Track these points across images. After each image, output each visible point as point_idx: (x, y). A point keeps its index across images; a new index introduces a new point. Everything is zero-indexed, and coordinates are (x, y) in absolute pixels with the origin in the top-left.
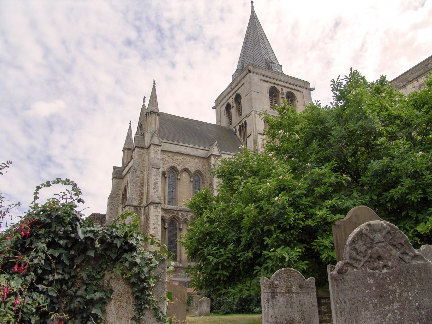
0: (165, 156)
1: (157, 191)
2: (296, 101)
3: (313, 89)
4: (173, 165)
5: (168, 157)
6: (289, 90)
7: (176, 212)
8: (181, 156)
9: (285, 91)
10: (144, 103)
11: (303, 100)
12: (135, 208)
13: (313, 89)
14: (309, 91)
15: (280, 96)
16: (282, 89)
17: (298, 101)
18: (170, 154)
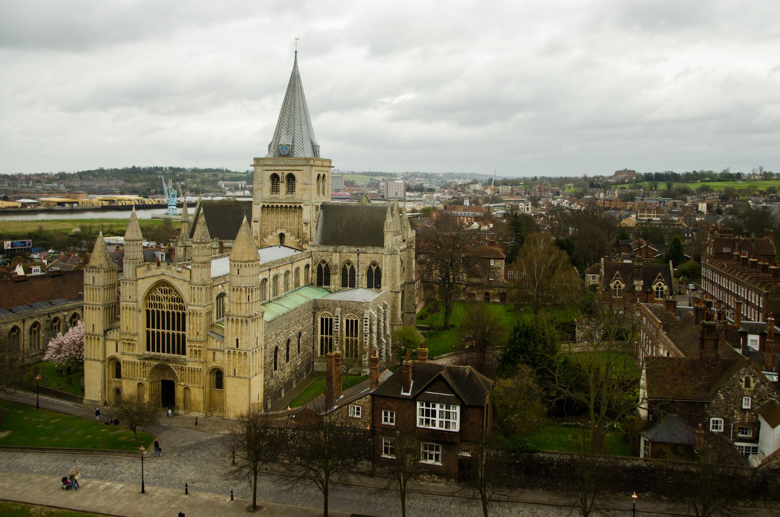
6: (289, 172)
9: (286, 173)
14: (309, 167)
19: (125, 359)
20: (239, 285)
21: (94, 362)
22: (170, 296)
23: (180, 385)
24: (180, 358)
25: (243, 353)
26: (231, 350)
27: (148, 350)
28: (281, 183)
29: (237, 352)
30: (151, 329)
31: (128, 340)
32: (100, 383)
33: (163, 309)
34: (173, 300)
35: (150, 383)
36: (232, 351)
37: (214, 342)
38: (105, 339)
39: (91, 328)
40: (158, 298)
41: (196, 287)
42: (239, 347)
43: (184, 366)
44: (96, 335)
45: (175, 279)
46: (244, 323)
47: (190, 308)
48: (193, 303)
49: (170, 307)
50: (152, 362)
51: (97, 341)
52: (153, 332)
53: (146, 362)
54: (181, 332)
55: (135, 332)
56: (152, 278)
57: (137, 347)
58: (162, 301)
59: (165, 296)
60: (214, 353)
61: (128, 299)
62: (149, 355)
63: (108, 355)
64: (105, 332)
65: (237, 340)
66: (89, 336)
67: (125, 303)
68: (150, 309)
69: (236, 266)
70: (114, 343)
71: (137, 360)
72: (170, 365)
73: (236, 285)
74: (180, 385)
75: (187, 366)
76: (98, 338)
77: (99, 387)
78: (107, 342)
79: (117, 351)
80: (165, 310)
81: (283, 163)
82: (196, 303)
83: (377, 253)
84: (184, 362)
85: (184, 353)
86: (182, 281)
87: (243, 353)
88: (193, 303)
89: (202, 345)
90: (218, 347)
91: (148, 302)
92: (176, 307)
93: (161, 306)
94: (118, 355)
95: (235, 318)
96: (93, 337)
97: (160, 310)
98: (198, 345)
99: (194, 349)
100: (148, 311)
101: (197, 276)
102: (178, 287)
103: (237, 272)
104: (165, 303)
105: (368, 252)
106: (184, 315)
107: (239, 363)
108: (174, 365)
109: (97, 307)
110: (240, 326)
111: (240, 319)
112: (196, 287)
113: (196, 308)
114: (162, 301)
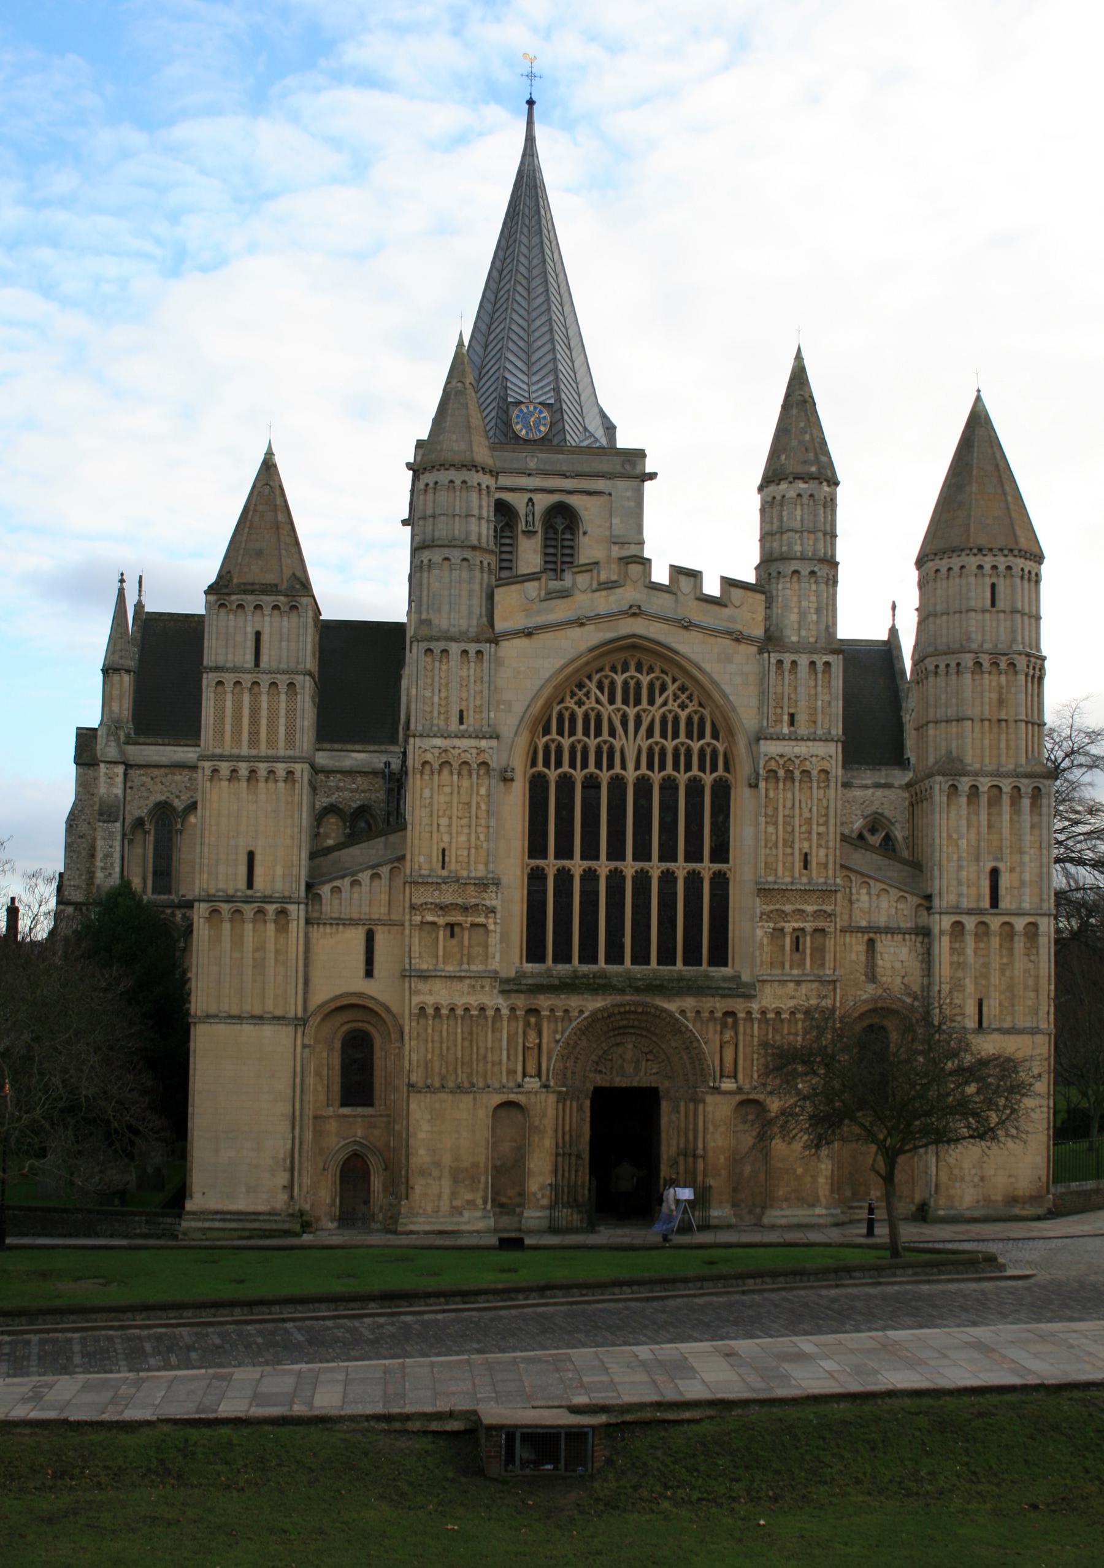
0: (144, 778)
1: (110, 874)
2: (581, 532)
3: (652, 476)
4: (163, 798)
5: (152, 779)
7: (169, 911)
8: (186, 772)
9: (543, 502)
10: (140, 596)
11: (608, 524)
12: (75, 909)
13: (652, 476)
14: (633, 483)
15: (522, 526)
16: (530, 500)
17: (585, 533)
18: (156, 772)
19: (430, 1000)
20: (1002, 647)
21: (247, 1029)
22: (656, 712)
23: (716, 1090)
24: (707, 976)
25: (1020, 924)
26: (964, 919)
27: (534, 952)
28: (520, 536)
29: (995, 923)
30: (551, 865)
31: (443, 908)
32: (284, 1127)
33: (617, 769)
34: (669, 726)
35: (561, 1098)
36: (970, 923)
37: (863, 899)
38: (308, 922)
39: (243, 870)
40: (594, 724)
41: (803, 661)
42: (1005, 903)
43: (739, 1006)
44: (267, 899)
45: (694, 636)
46: (1026, 803)
47: (770, 748)
48: (786, 730)
49: (654, 758)
50: (574, 1002)
51: (271, 927)
52: (564, 877)
53: (544, 1002)
54: (707, 868)
55: (480, 871)
56: (576, 633)
57: (494, 940)
58: (612, 733)
59: (631, 712)
60: (871, 943)
61: (454, 726)
62: (549, 974)
63: (323, 992)
64: (309, 886)
65: (995, 873)
66: (225, 907)
67: (438, 742)
68: (553, 775)
69: (987, 567)
70: (356, 937)
71: (492, 999)
72: (672, 1006)
73: (987, 646)
74: (716, 1090)
75: (755, 1006)
76: (282, 913)
77: (278, 1143)
78: (316, 933)
79: (369, 973)
80: (631, 775)
81: (532, 464)
82: (802, 730)
83: (888, 786)
84: (742, 990)
85: (720, 956)
86: (726, 643)
87: (1020, 924)
88: (786, 730)
89: (829, 908)
90: (882, 920)
91: (542, 742)
92: (682, 758)
93: (608, 756)
94: (380, 989)
95: (985, 783)
96: (249, 910)
97: (605, 776)
98: (809, 909)
99: (788, 927)
100: (537, 785)
101: (802, 615)
102: (707, 667)
103: (988, 595)
104: (631, 745)
105: (856, 782)
106: (722, 791)
107: (1002, 971)
108: (689, 1003)
109: (281, 769)
110: (1006, 817)
111: (1006, 785)
112: (803, 661)
113: (801, 749)
114: (612, 733)
